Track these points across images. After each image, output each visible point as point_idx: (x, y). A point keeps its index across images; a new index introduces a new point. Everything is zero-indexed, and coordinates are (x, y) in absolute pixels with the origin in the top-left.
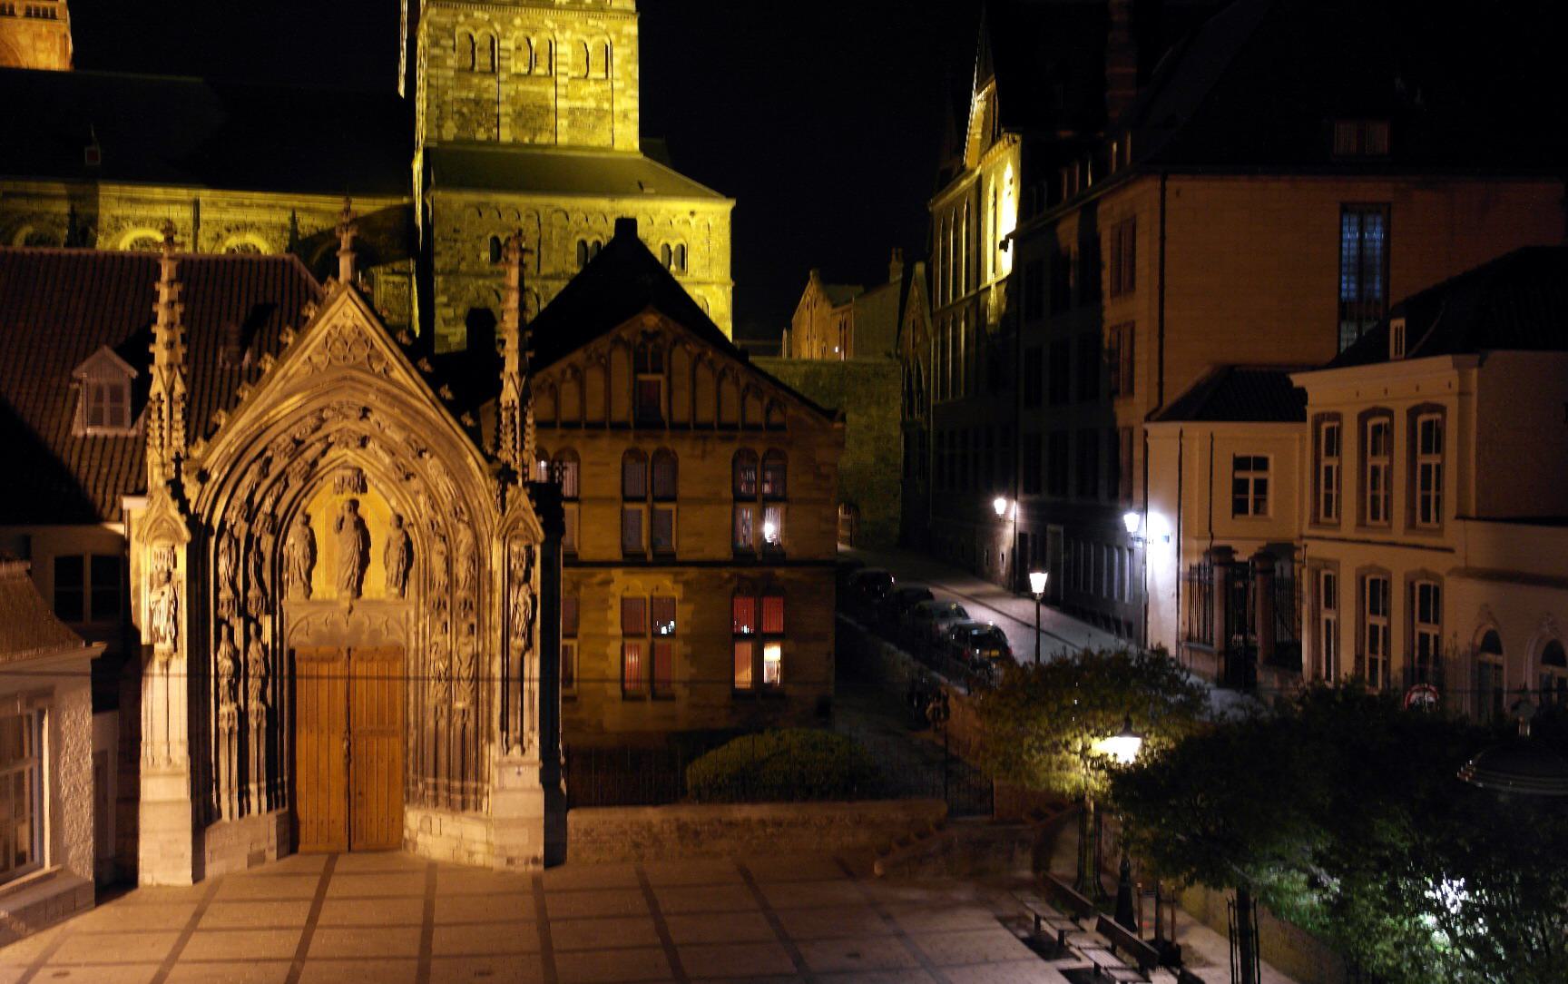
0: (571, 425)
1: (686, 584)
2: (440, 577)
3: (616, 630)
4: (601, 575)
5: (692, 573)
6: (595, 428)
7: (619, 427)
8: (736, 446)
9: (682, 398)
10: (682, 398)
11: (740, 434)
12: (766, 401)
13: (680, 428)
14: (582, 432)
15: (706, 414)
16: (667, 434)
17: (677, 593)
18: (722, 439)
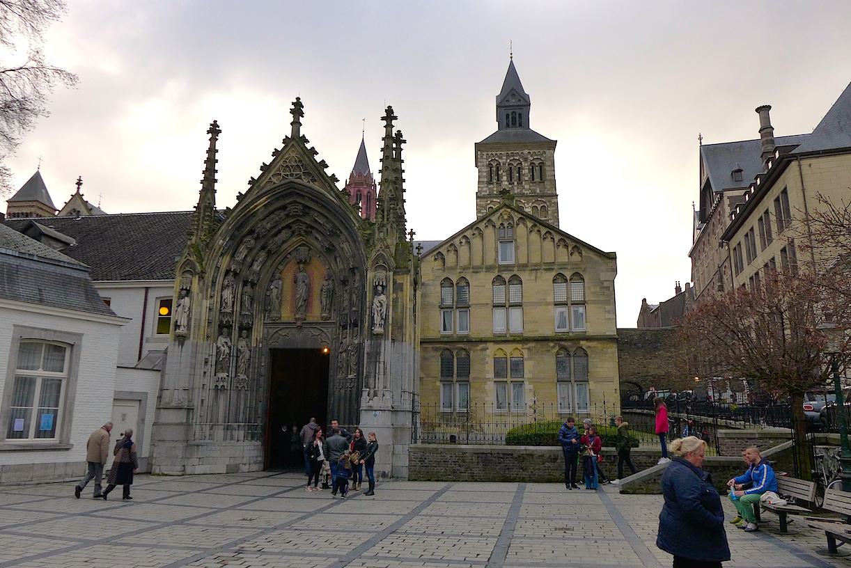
0: (465, 268)
1: (529, 349)
2: (346, 303)
3: (491, 375)
4: (481, 346)
5: (531, 345)
6: (476, 270)
7: (489, 269)
8: (554, 273)
9: (523, 249)
10: (523, 249)
11: (556, 267)
12: (570, 249)
13: (523, 267)
14: (471, 270)
15: (535, 259)
16: (516, 269)
17: (525, 353)
18: (546, 270)
